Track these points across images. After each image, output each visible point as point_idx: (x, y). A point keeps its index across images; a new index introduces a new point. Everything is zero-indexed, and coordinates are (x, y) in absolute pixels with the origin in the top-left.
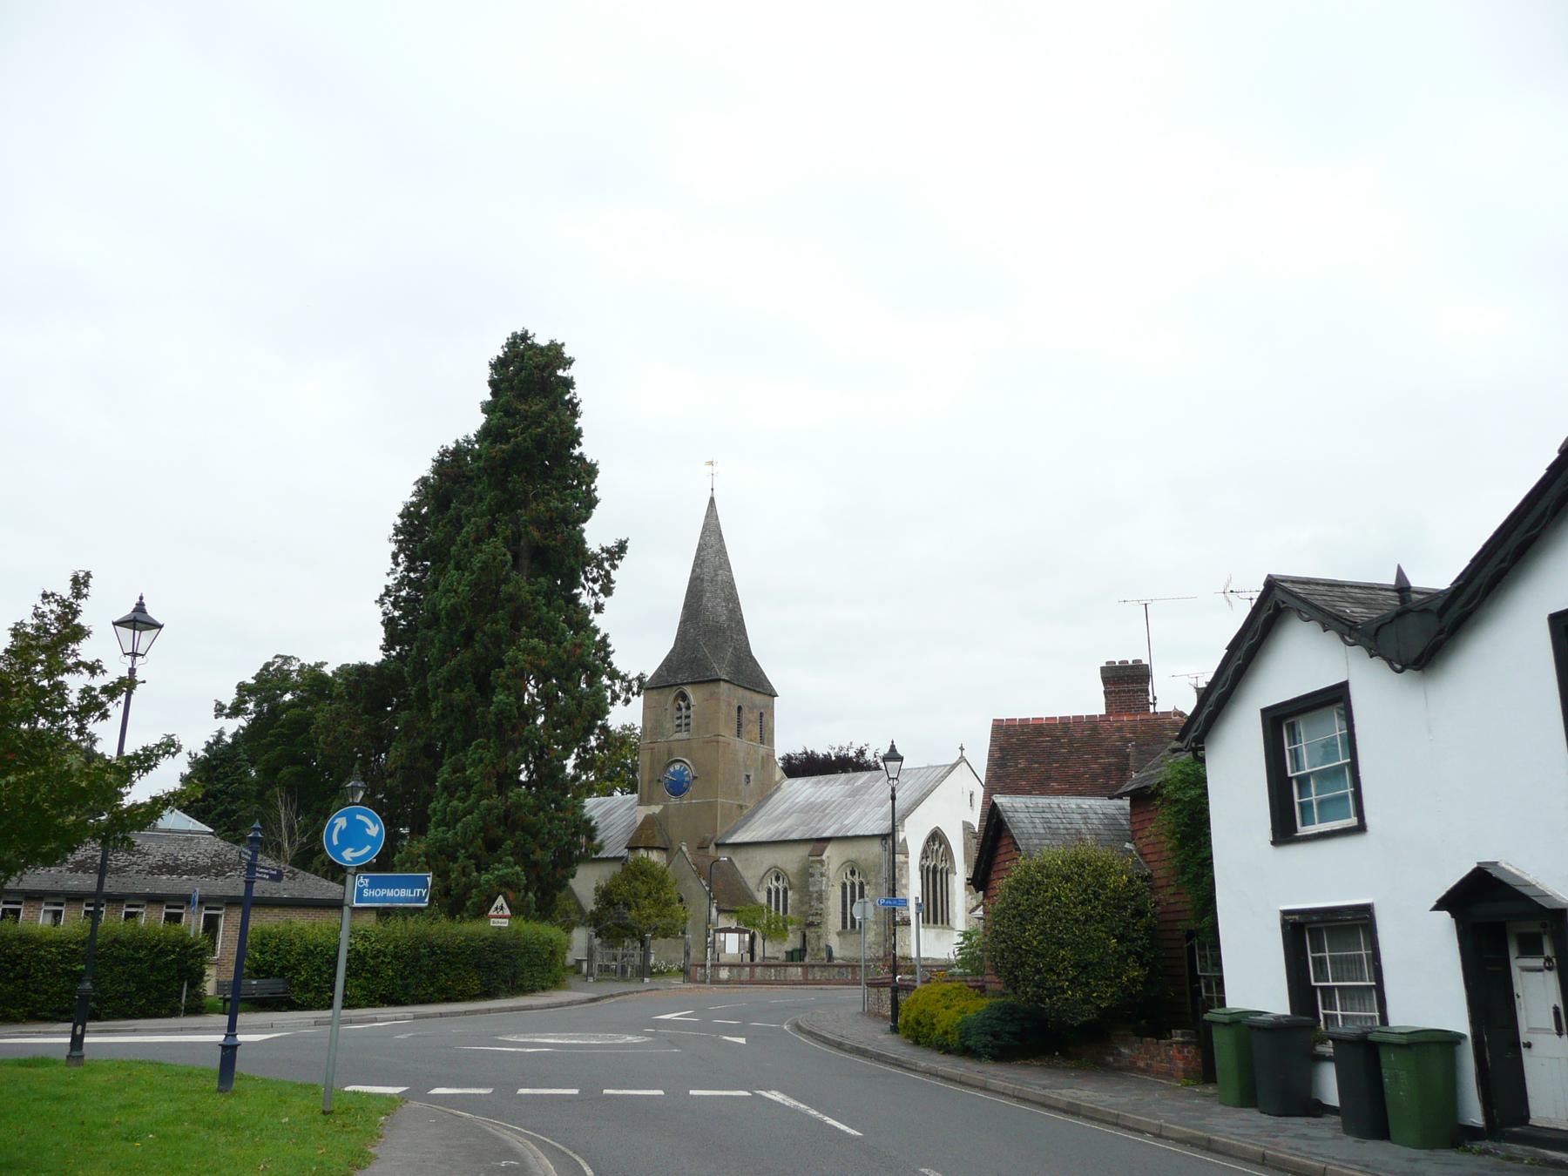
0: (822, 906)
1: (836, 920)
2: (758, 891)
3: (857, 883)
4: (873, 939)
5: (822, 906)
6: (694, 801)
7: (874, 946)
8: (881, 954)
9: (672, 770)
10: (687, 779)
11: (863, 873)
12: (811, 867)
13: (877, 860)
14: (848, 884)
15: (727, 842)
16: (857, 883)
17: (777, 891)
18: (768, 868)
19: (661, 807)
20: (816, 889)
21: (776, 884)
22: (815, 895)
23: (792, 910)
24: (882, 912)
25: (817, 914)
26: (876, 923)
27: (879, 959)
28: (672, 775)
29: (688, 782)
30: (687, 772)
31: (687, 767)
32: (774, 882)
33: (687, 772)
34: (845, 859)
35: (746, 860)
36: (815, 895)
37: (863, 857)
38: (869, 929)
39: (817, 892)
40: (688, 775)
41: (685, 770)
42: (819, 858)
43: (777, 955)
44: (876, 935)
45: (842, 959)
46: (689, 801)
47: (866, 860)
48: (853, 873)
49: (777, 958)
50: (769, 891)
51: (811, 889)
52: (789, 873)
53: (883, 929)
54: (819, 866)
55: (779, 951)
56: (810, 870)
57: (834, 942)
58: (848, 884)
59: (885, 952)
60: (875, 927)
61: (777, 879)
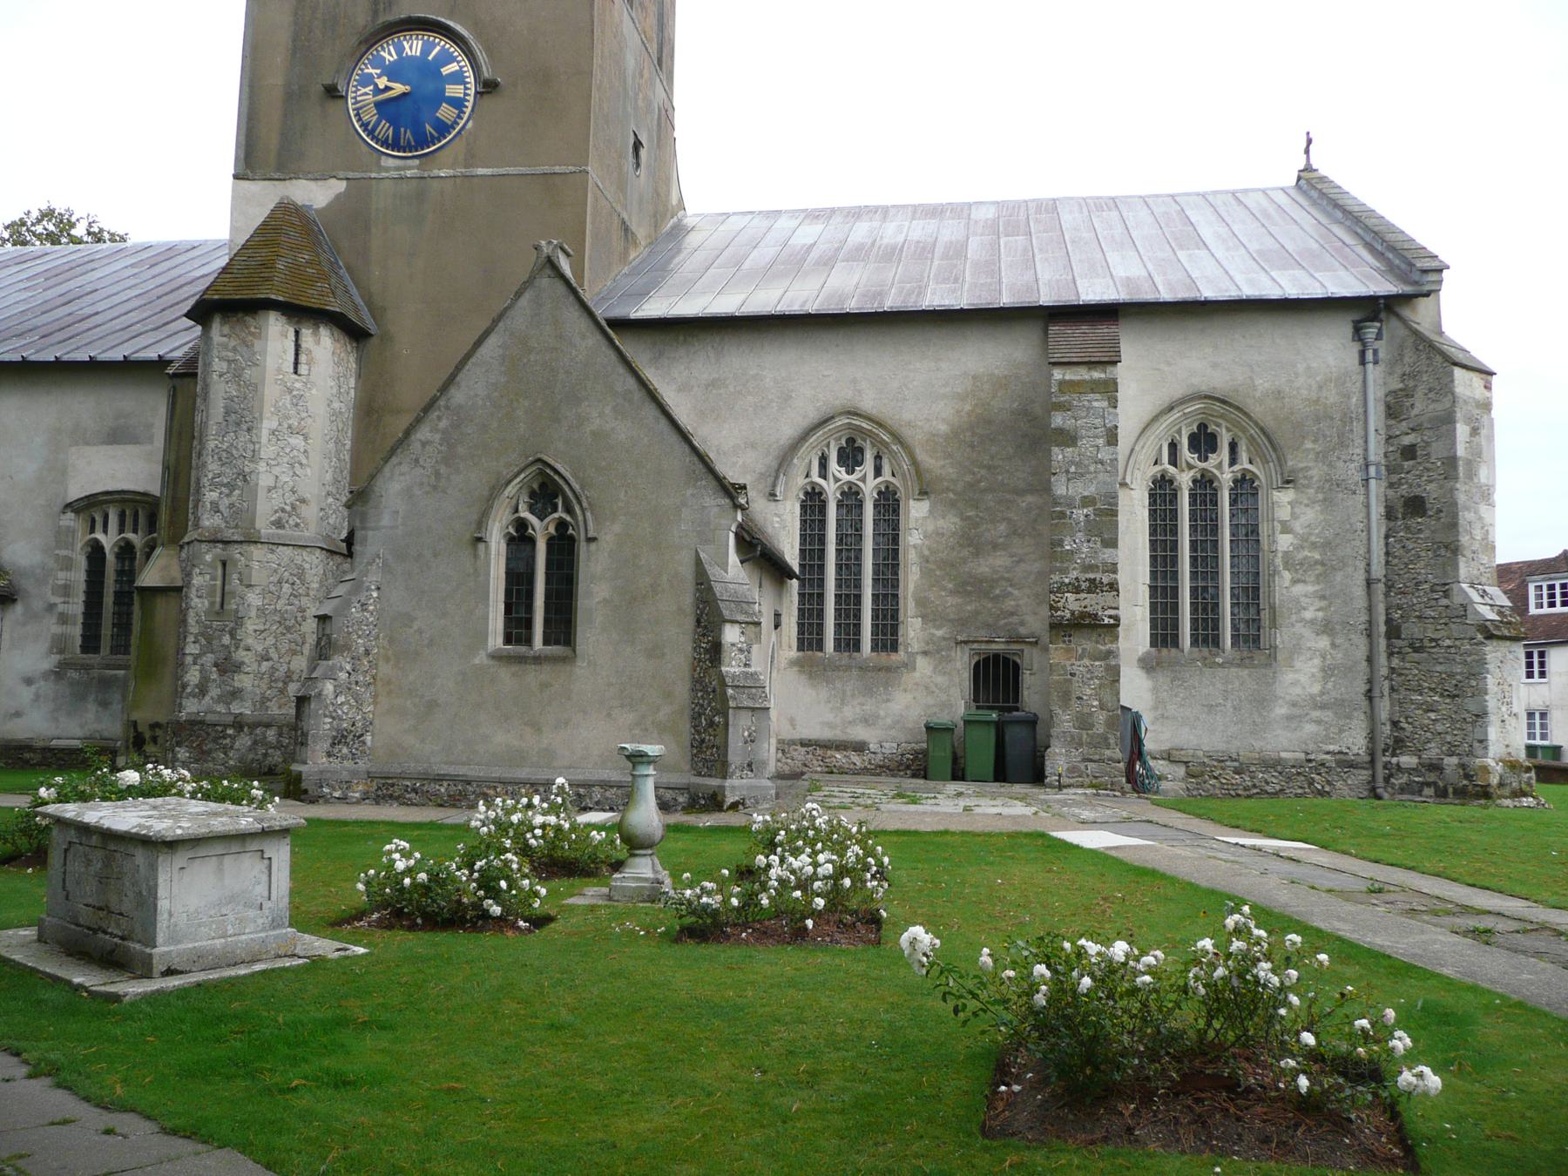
0: (1107, 555)
1: (1139, 610)
2: (772, 495)
3: (1226, 477)
4: (1316, 689)
5: (1107, 555)
6: (481, 171)
7: (1316, 714)
8: (1355, 741)
9: (389, 54)
10: (454, 90)
11: (1269, 443)
12: (1061, 407)
13: (1331, 396)
14: (1184, 480)
15: (633, 316)
16: (1226, 477)
17: (851, 498)
18: (813, 416)
19: (340, 186)
20: (1080, 489)
21: (845, 477)
22: (1080, 514)
23: (926, 573)
24: (1359, 591)
25: (1094, 586)
26: (1326, 628)
27: (1347, 764)
28: (393, 72)
29: (458, 103)
30: (453, 67)
31: (454, 50)
32: (833, 465)
33: (453, 67)
34: (1178, 392)
35: (713, 384)
36: (1080, 514)
37: (1263, 383)
38: (1296, 649)
39: (1087, 501)
40: (458, 78)
41: (447, 58)
42: (1097, 375)
43: (859, 733)
44: (1328, 671)
45: (1168, 757)
46: (460, 170)
47: (1278, 394)
48: (1203, 441)
49: (860, 747)
50: (813, 503)
51: (1060, 488)
52: (915, 437)
53: (1361, 652)
54: (1100, 404)
55: (867, 721)
56: (1058, 420)
57: (1135, 690)
58: (1184, 480)
59: (1372, 737)
60: (1324, 642)
61: (851, 456)
